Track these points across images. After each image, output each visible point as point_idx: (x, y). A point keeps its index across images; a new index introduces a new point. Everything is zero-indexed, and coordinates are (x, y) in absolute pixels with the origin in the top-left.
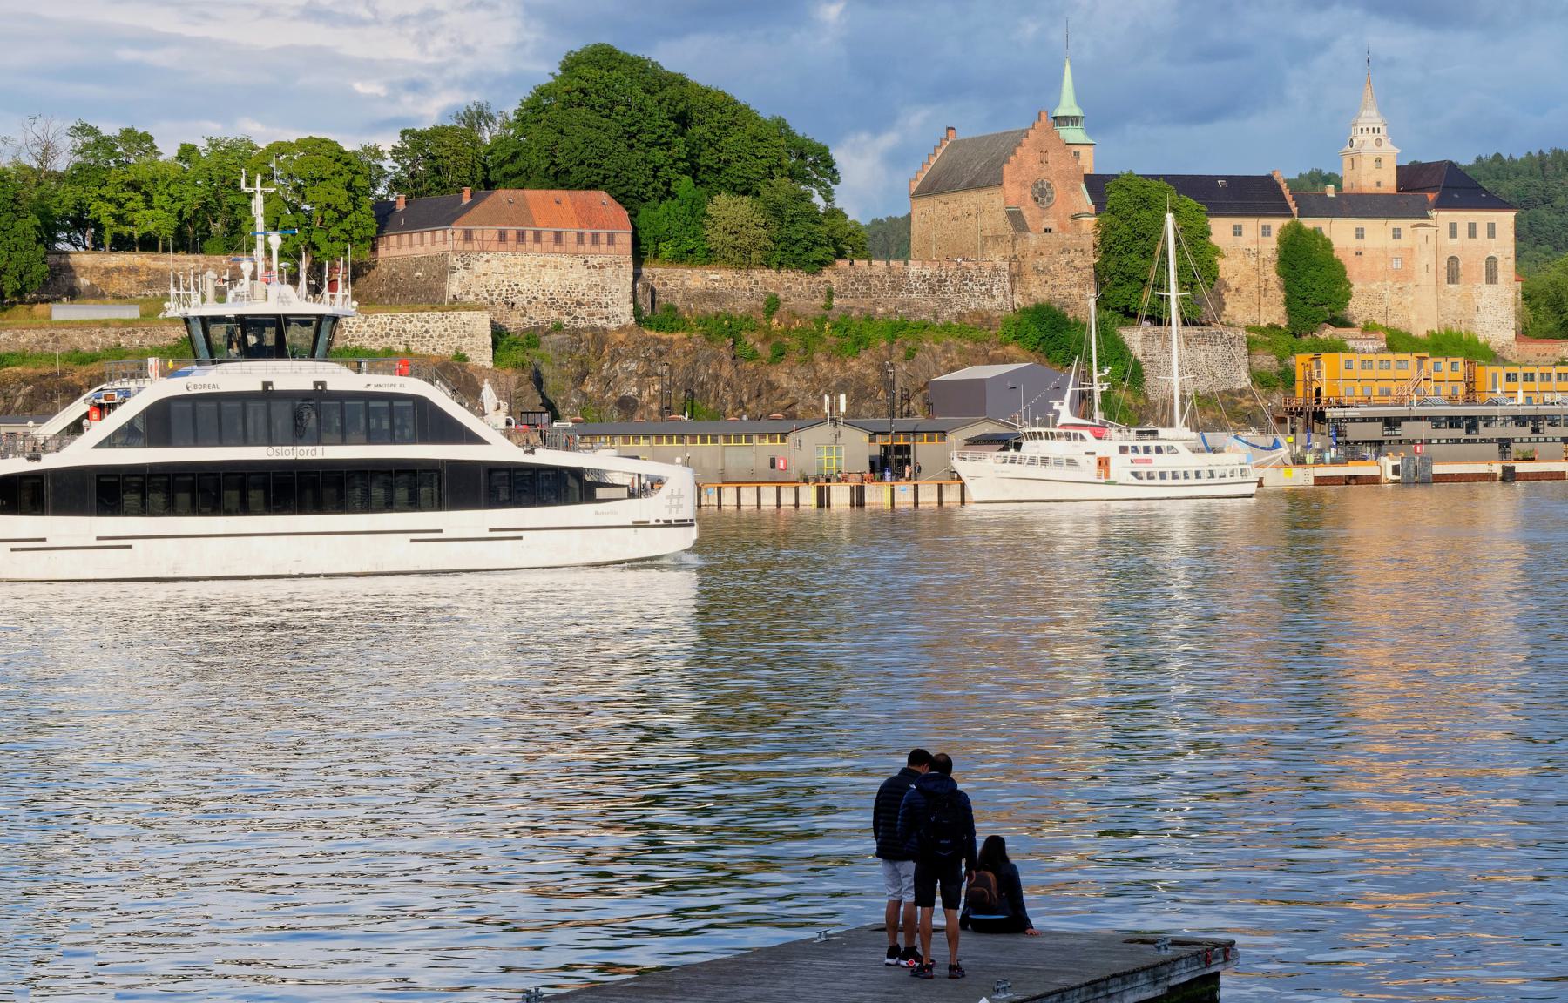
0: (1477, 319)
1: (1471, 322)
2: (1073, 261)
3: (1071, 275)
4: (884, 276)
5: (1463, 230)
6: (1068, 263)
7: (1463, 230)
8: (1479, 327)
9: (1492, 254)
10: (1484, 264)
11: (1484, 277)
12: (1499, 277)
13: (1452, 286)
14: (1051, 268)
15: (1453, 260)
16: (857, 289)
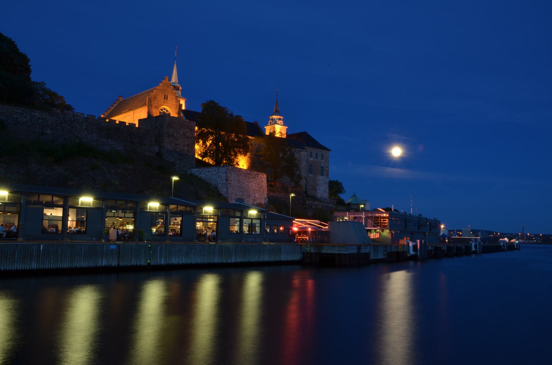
0: (318, 188)
1: (316, 189)
2: (186, 133)
3: (184, 140)
4: (82, 122)
5: (314, 155)
6: (183, 133)
7: (314, 155)
8: (318, 191)
9: (323, 165)
10: (320, 168)
11: (320, 173)
12: (325, 173)
13: (310, 175)
14: (175, 134)
15: (311, 165)
16: (64, 127)
